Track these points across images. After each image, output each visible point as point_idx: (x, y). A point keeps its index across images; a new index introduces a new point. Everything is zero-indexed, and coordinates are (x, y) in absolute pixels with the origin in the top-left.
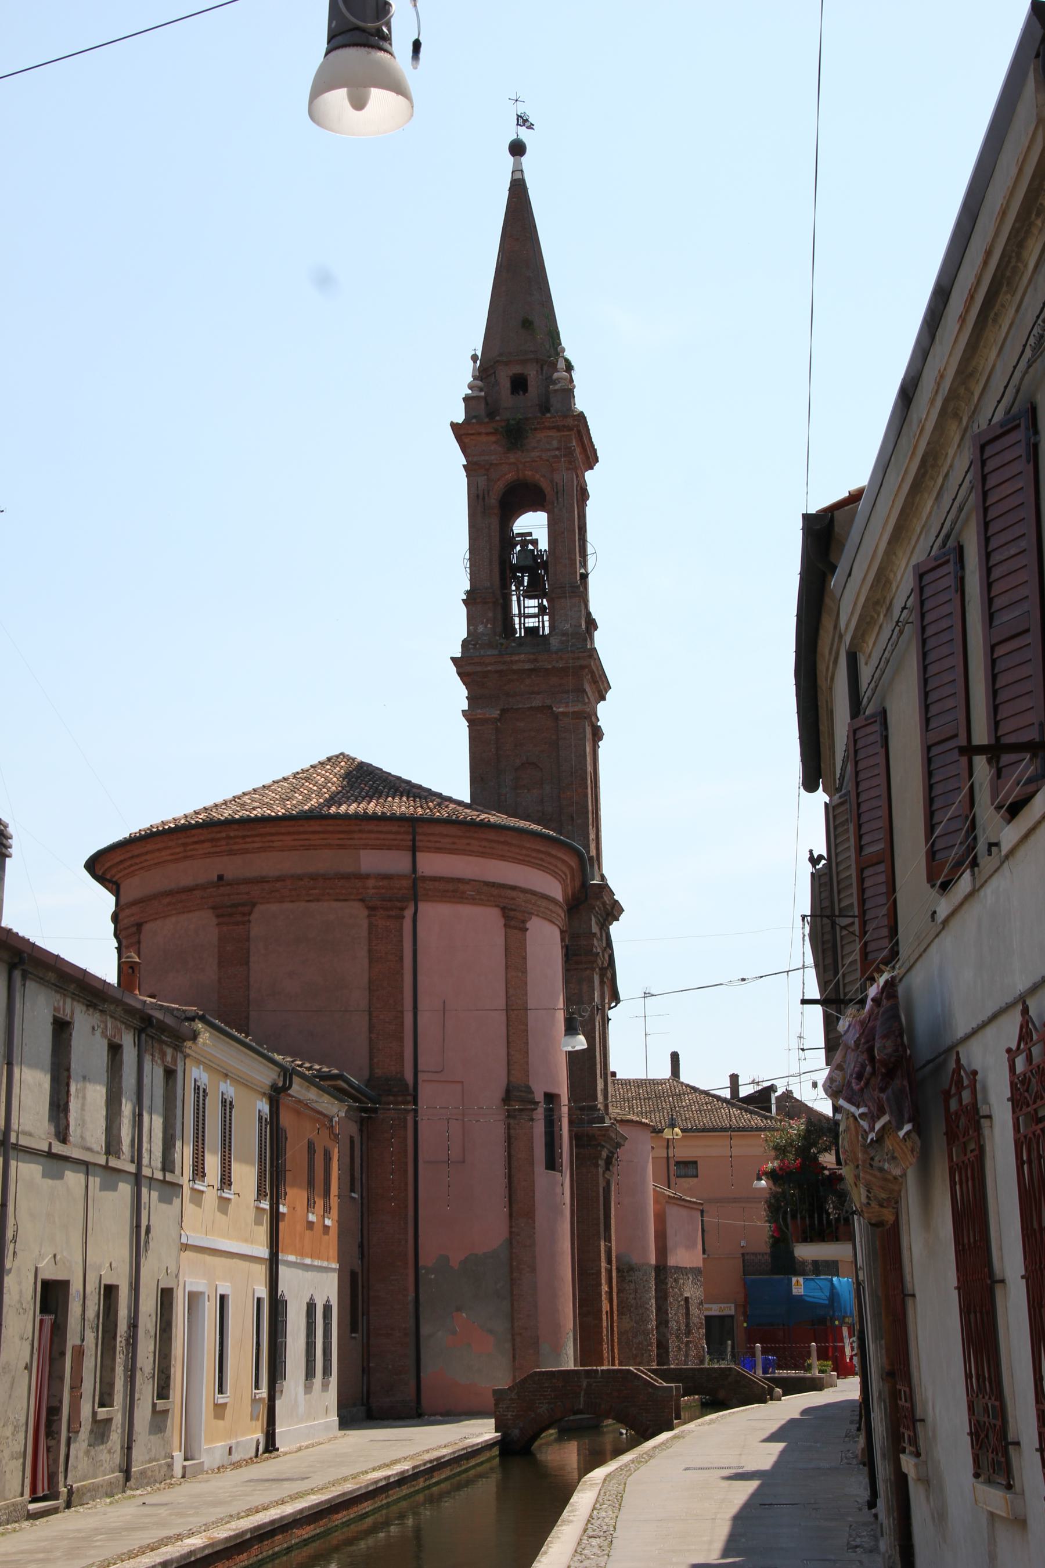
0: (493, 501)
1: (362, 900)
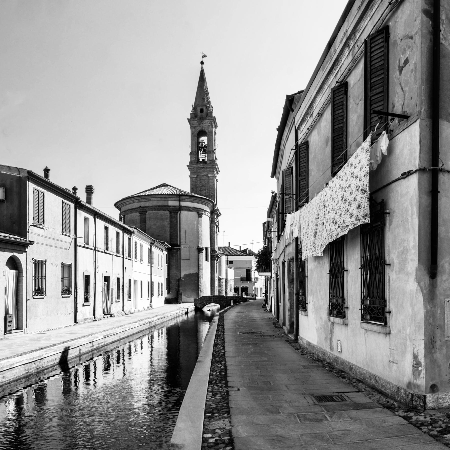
1: (169, 210)
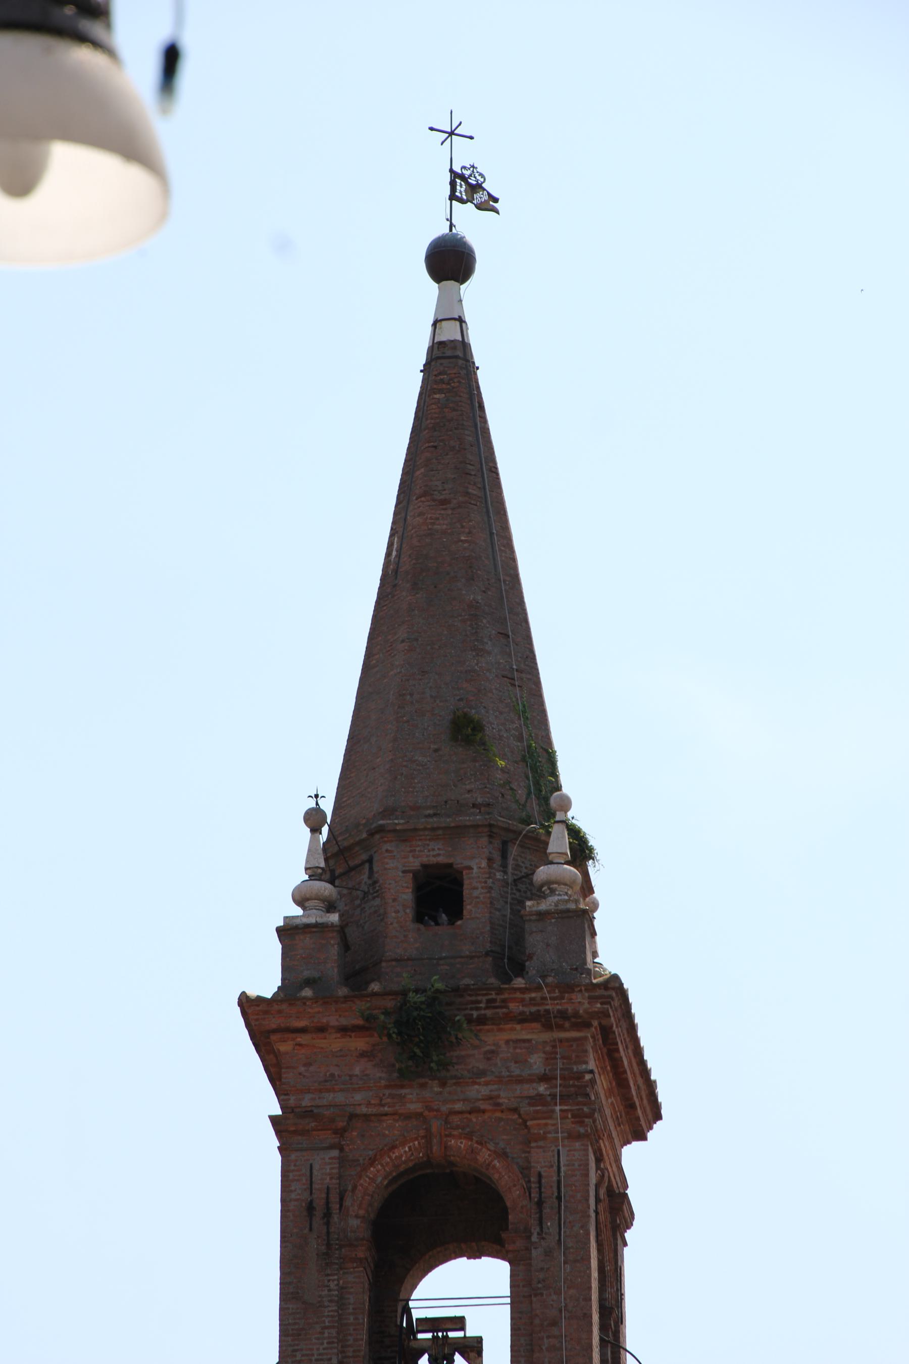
0: (354, 1223)
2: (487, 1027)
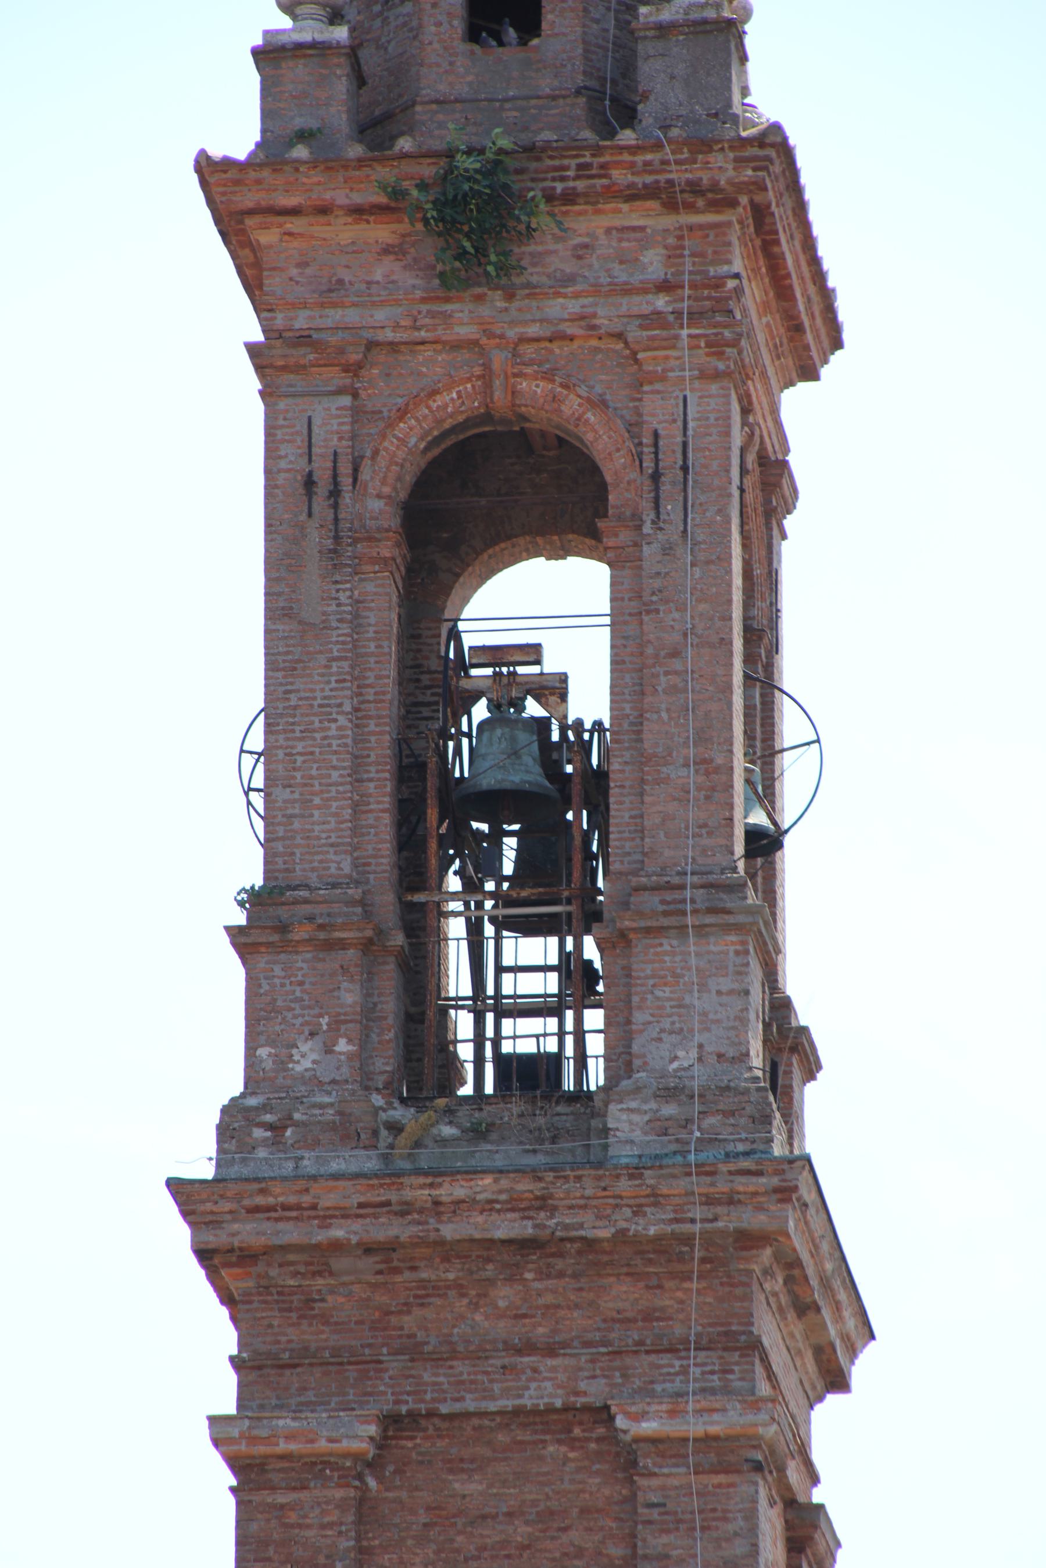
0: (376, 505)
2: (577, 208)
